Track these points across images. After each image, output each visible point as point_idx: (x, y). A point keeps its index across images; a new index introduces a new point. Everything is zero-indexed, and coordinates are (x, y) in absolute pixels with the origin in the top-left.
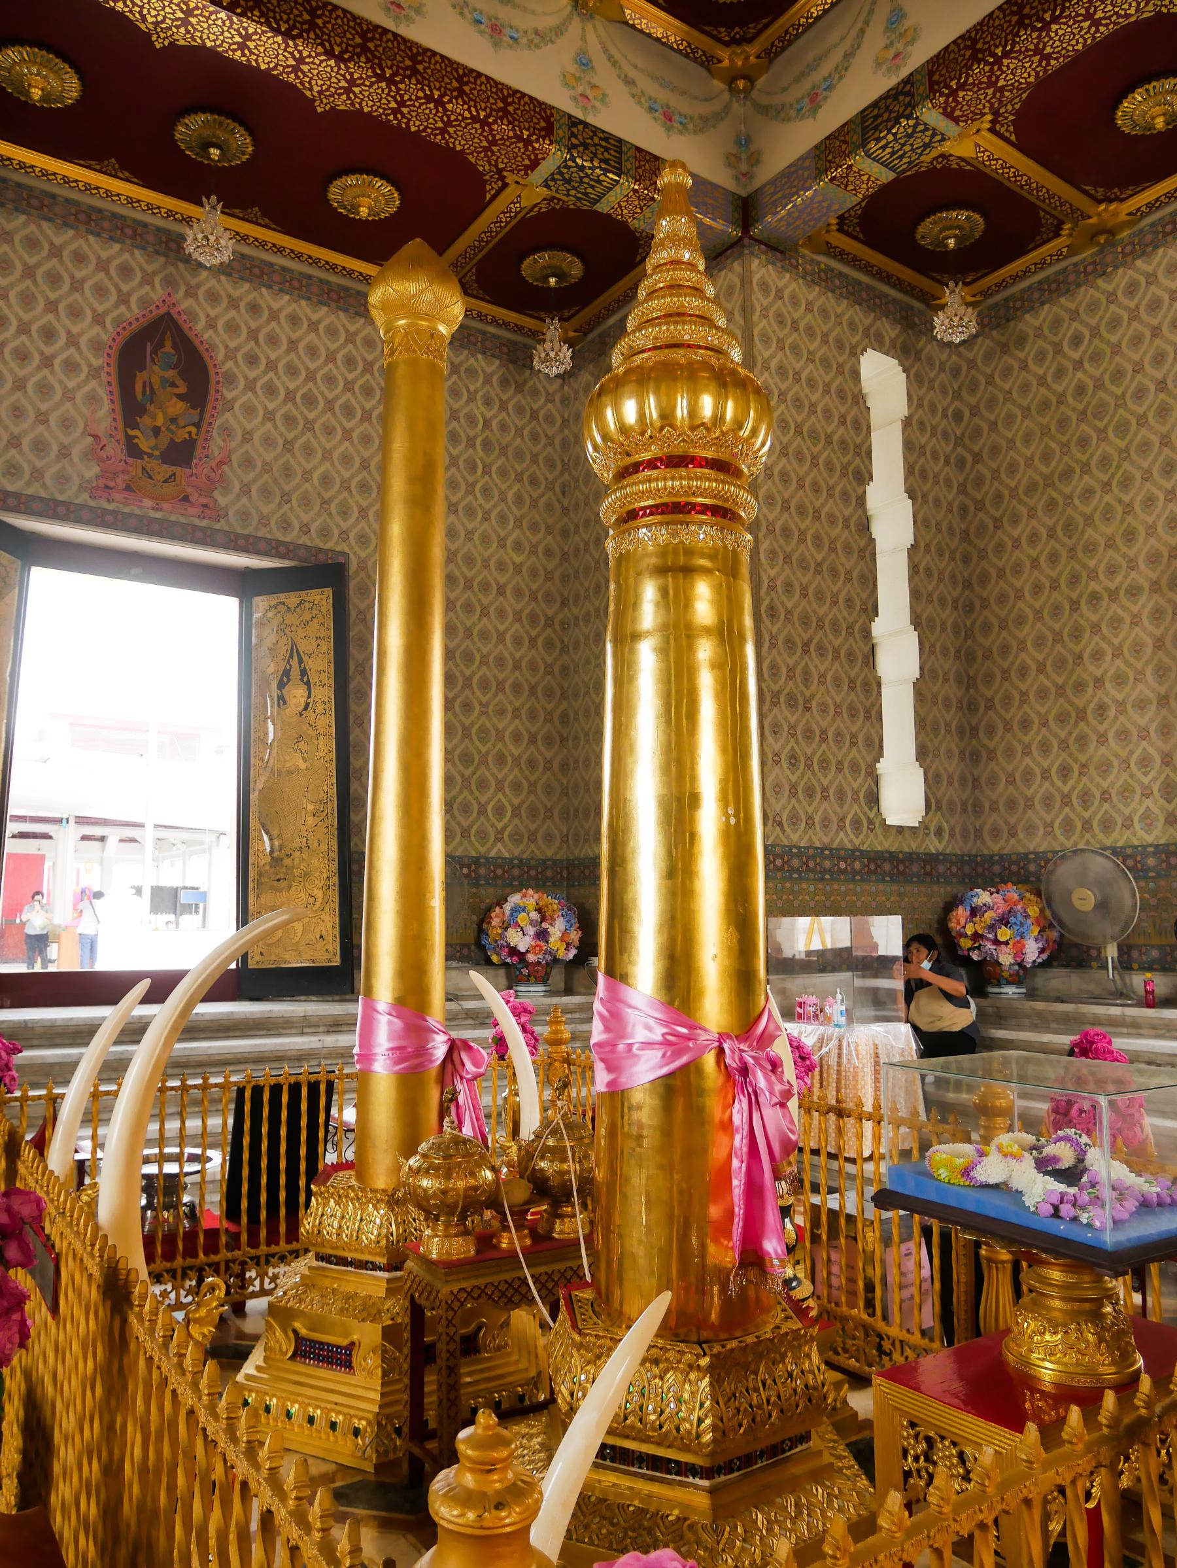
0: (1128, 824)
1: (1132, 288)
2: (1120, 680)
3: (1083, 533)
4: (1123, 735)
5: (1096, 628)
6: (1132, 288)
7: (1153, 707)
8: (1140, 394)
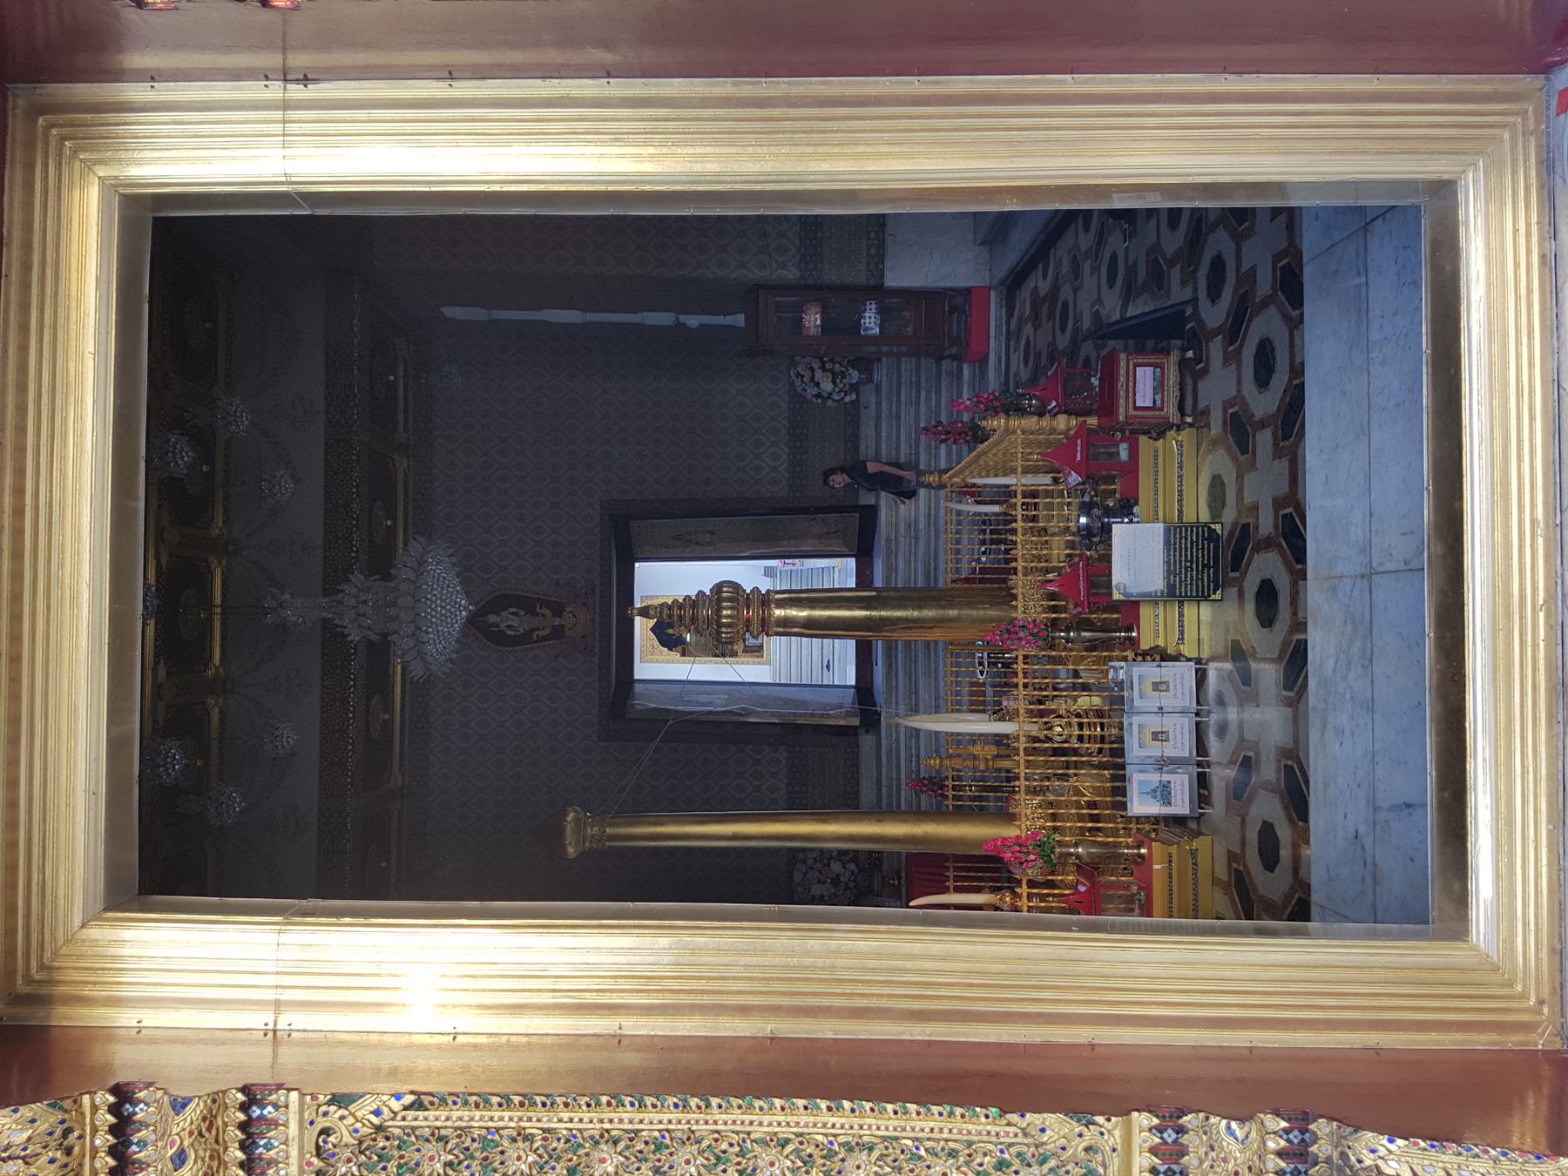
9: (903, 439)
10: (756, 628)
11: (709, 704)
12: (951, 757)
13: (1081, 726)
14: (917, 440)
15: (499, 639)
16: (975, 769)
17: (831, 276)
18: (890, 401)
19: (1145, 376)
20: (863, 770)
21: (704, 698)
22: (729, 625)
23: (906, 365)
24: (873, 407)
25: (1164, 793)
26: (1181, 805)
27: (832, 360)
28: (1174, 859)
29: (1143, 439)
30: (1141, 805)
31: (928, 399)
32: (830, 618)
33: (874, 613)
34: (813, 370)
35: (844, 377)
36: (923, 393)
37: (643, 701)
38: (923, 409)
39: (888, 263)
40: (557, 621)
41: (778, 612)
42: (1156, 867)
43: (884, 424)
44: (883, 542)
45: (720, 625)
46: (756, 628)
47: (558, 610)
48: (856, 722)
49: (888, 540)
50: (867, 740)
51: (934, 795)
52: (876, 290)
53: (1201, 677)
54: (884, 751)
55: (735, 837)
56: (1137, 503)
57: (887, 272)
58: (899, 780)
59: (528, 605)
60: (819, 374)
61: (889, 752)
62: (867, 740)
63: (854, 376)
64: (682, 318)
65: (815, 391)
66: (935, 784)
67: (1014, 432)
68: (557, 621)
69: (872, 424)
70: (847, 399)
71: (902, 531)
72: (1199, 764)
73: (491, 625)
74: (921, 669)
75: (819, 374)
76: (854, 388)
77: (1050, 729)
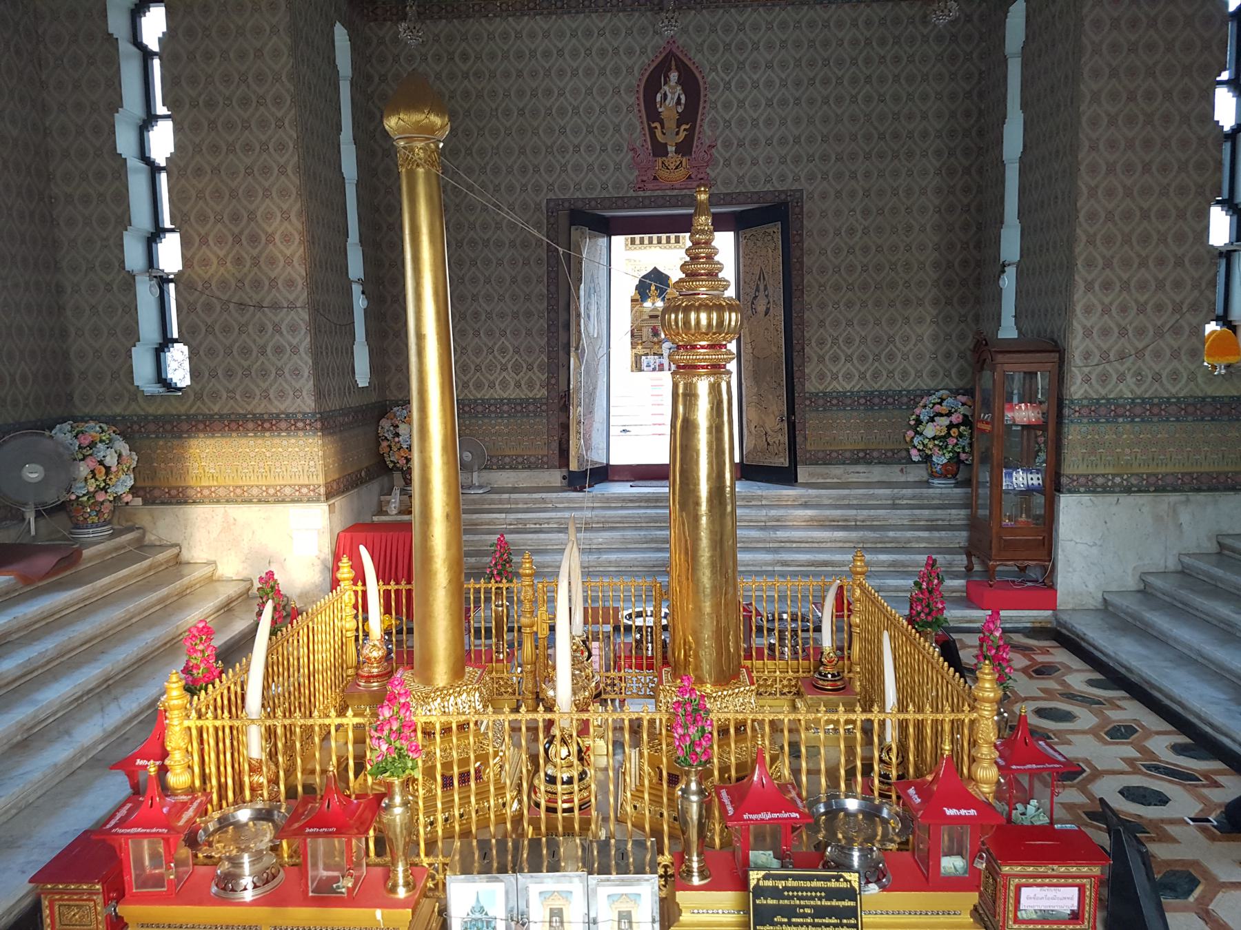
1: (505, 36)
2: (488, 298)
4: (490, 333)
5: (474, 263)
6: (505, 36)
7: (509, 319)
8: (507, 113)
9: (872, 512)
10: (685, 357)
13: (570, 781)
14: (919, 551)
17: (1074, 434)
18: (913, 498)
19: (1064, 899)
20: (525, 474)
21: (593, 313)
22: (686, 322)
23: (958, 515)
24: (903, 479)
27: (961, 435)
29: (973, 898)
31: (919, 539)
33: (704, 507)
34: (949, 414)
35: (941, 448)
36: (925, 534)
37: (592, 248)
38: (909, 534)
39: (1086, 498)
40: (671, 149)
41: (703, 386)
43: (888, 491)
44: (759, 492)
45: (687, 310)
46: (685, 357)
47: (684, 148)
48: (574, 466)
49: (761, 498)
50: (555, 477)
51: (490, 566)
52: (1054, 486)
54: (544, 495)
55: (420, 337)
56: (884, 888)
57: (1075, 497)
59: (689, 115)
60: (945, 421)
61: (544, 500)
62: (555, 477)
63: (940, 459)
64: (1011, 272)
65: (924, 418)
66: (502, 565)
67: (973, 709)
68: (671, 149)
69: (885, 478)
70: (914, 452)
71: (773, 512)
73: (667, 77)
74: (629, 534)
75: (945, 421)
76: (927, 459)
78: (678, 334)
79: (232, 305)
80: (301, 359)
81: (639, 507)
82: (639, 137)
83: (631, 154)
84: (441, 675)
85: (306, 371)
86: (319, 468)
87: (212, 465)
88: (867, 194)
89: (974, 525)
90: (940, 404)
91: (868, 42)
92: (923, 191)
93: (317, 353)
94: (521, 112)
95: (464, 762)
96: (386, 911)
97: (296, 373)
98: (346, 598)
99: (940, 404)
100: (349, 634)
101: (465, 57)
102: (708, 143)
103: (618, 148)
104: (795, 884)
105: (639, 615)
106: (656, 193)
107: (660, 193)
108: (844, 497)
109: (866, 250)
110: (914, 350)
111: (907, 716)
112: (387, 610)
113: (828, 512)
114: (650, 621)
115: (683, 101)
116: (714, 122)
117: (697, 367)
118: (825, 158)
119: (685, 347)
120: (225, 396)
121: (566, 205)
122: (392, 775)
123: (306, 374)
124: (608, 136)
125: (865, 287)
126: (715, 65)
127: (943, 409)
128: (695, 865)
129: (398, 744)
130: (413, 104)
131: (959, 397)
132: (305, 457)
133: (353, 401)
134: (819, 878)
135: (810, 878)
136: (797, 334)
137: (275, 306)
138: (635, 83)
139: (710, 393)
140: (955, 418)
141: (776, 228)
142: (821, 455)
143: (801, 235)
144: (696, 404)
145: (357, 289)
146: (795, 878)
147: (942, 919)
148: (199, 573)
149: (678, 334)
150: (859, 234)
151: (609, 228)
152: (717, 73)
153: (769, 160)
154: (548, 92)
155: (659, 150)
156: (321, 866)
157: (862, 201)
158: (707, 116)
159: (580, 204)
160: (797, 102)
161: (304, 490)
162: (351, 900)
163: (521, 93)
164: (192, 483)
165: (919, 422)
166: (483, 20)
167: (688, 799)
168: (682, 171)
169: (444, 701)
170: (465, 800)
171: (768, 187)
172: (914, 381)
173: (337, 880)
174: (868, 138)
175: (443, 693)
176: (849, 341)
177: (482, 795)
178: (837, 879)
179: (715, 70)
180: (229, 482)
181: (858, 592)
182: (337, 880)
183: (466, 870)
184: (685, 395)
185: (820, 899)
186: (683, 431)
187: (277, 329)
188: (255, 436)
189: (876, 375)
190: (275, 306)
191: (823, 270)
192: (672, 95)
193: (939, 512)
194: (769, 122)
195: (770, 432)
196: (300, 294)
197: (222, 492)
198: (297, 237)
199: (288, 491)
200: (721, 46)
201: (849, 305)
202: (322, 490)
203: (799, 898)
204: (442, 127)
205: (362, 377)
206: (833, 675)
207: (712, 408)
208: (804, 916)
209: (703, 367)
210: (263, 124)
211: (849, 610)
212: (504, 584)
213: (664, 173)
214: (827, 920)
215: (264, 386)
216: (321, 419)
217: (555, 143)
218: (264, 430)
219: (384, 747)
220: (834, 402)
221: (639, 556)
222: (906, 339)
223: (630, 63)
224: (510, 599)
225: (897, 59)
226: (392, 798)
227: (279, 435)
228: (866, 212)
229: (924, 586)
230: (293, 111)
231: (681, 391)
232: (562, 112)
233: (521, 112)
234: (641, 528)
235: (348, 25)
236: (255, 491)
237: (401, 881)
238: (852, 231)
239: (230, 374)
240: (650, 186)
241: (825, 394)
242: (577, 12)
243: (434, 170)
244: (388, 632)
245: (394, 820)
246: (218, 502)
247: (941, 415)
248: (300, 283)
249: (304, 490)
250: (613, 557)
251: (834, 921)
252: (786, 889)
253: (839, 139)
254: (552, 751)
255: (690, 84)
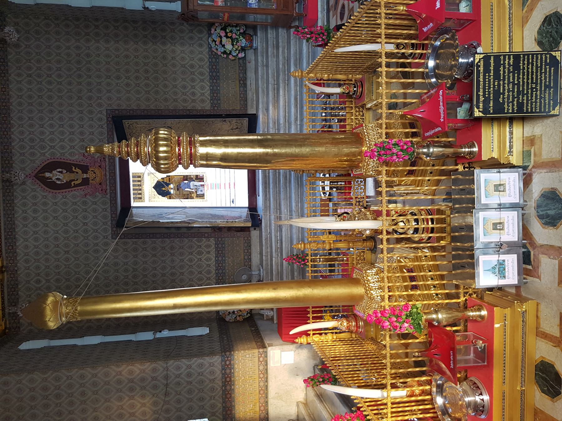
0: (209, 266)
3: (110, 280)
4: (182, 267)
5: (145, 276)
6: (27, 261)
8: (67, 260)
9: (270, 76)
10: (185, 159)
11: (172, 218)
12: (310, 243)
13: (417, 221)
15: (52, 185)
16: (324, 249)
18: (263, 56)
20: (253, 248)
21: (171, 216)
22: (165, 158)
23: (271, 34)
25: (500, 269)
26: (512, 278)
27: (231, 32)
28: (508, 318)
30: (485, 279)
32: (239, 153)
33: (269, 150)
35: (237, 42)
38: (281, 58)
40: (85, 176)
41: (202, 150)
42: (497, 326)
43: (260, 69)
45: (158, 158)
46: (185, 159)
47: (85, 169)
48: (249, 224)
50: (254, 234)
53: (527, 181)
54: (264, 239)
55: (175, 307)
56: (479, 45)
58: (271, 252)
59: (67, 167)
60: (224, 40)
61: (266, 239)
63: (243, 42)
65: (223, 50)
66: (300, 258)
68: (85, 176)
69: (253, 71)
71: (271, 125)
72: (524, 246)
73: (48, 178)
74: (282, 196)
75: (224, 40)
76: (243, 49)
77: (396, 224)
78: (172, 163)
79: (166, 399)
80: (194, 364)
81: (269, 192)
82: (78, 192)
83: (87, 196)
84: (358, 290)
85: (200, 361)
86: (250, 352)
87: (248, 406)
88: (109, 77)
89: (275, 25)
90: (215, 42)
91: (30, 75)
92: (107, 49)
93: (190, 356)
94: (67, 252)
95: (404, 279)
96: (495, 322)
97: (201, 365)
98: (316, 339)
99: (215, 42)
100: (335, 337)
101: (38, 281)
102: (82, 157)
103: (85, 203)
104: (481, 90)
105: (323, 188)
106: (108, 183)
107: (108, 182)
108: (263, 91)
109: (137, 78)
110: (189, 55)
111: (383, 33)
112: (321, 318)
113: (271, 98)
114: (327, 183)
115: (60, 170)
116: (71, 154)
117: (191, 153)
118: (90, 98)
119: (180, 160)
120: (213, 401)
121: (115, 229)
122: (421, 320)
123: (202, 361)
124: (79, 208)
125: (156, 79)
126: (41, 154)
127: (218, 40)
128: (467, 150)
129: (404, 317)
130: (41, 314)
131: (212, 32)
132: (244, 360)
133: (216, 335)
134: (478, 77)
135: (478, 81)
136: (181, 113)
137: (166, 377)
138: (51, 195)
139: (206, 146)
140: (223, 34)
141: (126, 123)
142: (242, 102)
143: (130, 110)
144: (212, 154)
145: (158, 335)
146: (478, 90)
147: (495, 13)
148: (303, 412)
149: (172, 163)
150: (129, 81)
151: (126, 207)
152: (46, 152)
153: (91, 126)
154: (56, 239)
155: (86, 182)
156: (468, 357)
157: (112, 80)
158: (68, 158)
159: (114, 222)
160: (60, 112)
161: (261, 359)
162: (489, 341)
163: (57, 253)
164: (257, 415)
165: (225, 53)
166: (19, 272)
167: (432, 153)
168: (96, 170)
169: (376, 289)
170: (424, 278)
171: (105, 126)
172: (204, 55)
173: (476, 350)
174: (80, 76)
175: (368, 289)
176: (184, 87)
177: (421, 268)
178: (478, 66)
179: (44, 154)
180: (257, 397)
181: (312, 75)
182: (476, 350)
183: (472, 277)
184: (207, 160)
185: (489, 76)
186: (227, 162)
187: (178, 376)
188: (233, 385)
189: (202, 74)
190: (166, 377)
191: (148, 100)
192: (57, 176)
193: (269, 43)
194: (71, 126)
195: (230, 128)
196: (160, 365)
197: (262, 400)
198: (130, 367)
199: (261, 368)
200: (31, 150)
201: (166, 86)
202: (261, 350)
203: (489, 88)
204: (55, 296)
205: (204, 331)
206: (355, 87)
207: (214, 145)
208: (499, 85)
209: (191, 150)
210: (70, 386)
211: (321, 80)
212: (309, 258)
213: (98, 179)
214: (502, 72)
215: (208, 381)
216: (225, 352)
217: (82, 235)
218: (230, 380)
219: (406, 325)
220: (215, 95)
221: (293, 191)
222: (183, 59)
223: (40, 197)
224: (316, 255)
225: (39, 61)
226: (433, 320)
227: (233, 373)
228: (118, 78)
229: (309, 36)
230: (63, 371)
231: (205, 162)
232: (66, 232)
233: (67, 252)
234: (279, 191)
235: (21, 342)
236: (262, 384)
237: (478, 313)
238: (128, 85)
239: (202, 399)
240: (104, 187)
241: (211, 100)
242: (14, 224)
243: (79, 301)
244: (333, 317)
245: (445, 318)
246: (267, 402)
247: (221, 41)
248: (154, 365)
249: (261, 359)
250: (294, 204)
251: (502, 68)
252: (484, 95)
253: (80, 91)
254: (401, 231)
255: (52, 166)
